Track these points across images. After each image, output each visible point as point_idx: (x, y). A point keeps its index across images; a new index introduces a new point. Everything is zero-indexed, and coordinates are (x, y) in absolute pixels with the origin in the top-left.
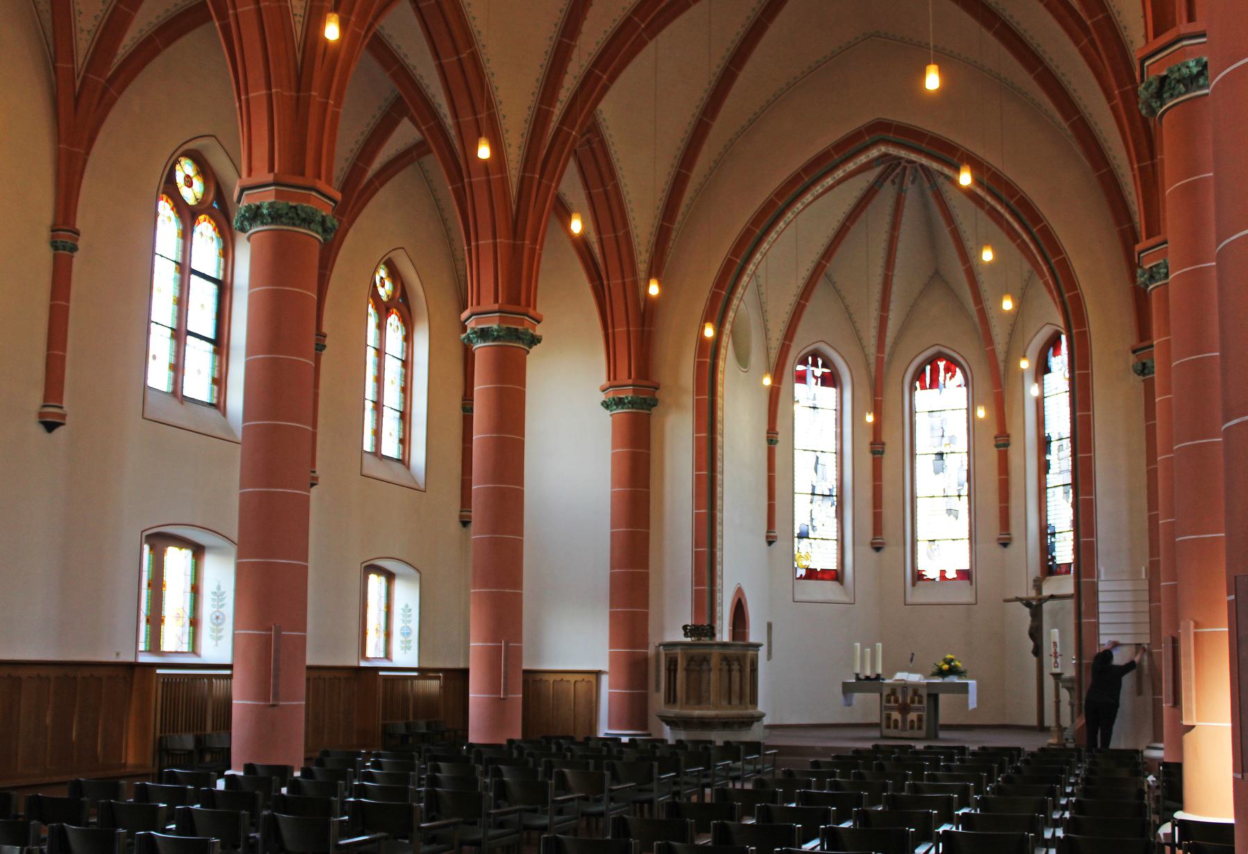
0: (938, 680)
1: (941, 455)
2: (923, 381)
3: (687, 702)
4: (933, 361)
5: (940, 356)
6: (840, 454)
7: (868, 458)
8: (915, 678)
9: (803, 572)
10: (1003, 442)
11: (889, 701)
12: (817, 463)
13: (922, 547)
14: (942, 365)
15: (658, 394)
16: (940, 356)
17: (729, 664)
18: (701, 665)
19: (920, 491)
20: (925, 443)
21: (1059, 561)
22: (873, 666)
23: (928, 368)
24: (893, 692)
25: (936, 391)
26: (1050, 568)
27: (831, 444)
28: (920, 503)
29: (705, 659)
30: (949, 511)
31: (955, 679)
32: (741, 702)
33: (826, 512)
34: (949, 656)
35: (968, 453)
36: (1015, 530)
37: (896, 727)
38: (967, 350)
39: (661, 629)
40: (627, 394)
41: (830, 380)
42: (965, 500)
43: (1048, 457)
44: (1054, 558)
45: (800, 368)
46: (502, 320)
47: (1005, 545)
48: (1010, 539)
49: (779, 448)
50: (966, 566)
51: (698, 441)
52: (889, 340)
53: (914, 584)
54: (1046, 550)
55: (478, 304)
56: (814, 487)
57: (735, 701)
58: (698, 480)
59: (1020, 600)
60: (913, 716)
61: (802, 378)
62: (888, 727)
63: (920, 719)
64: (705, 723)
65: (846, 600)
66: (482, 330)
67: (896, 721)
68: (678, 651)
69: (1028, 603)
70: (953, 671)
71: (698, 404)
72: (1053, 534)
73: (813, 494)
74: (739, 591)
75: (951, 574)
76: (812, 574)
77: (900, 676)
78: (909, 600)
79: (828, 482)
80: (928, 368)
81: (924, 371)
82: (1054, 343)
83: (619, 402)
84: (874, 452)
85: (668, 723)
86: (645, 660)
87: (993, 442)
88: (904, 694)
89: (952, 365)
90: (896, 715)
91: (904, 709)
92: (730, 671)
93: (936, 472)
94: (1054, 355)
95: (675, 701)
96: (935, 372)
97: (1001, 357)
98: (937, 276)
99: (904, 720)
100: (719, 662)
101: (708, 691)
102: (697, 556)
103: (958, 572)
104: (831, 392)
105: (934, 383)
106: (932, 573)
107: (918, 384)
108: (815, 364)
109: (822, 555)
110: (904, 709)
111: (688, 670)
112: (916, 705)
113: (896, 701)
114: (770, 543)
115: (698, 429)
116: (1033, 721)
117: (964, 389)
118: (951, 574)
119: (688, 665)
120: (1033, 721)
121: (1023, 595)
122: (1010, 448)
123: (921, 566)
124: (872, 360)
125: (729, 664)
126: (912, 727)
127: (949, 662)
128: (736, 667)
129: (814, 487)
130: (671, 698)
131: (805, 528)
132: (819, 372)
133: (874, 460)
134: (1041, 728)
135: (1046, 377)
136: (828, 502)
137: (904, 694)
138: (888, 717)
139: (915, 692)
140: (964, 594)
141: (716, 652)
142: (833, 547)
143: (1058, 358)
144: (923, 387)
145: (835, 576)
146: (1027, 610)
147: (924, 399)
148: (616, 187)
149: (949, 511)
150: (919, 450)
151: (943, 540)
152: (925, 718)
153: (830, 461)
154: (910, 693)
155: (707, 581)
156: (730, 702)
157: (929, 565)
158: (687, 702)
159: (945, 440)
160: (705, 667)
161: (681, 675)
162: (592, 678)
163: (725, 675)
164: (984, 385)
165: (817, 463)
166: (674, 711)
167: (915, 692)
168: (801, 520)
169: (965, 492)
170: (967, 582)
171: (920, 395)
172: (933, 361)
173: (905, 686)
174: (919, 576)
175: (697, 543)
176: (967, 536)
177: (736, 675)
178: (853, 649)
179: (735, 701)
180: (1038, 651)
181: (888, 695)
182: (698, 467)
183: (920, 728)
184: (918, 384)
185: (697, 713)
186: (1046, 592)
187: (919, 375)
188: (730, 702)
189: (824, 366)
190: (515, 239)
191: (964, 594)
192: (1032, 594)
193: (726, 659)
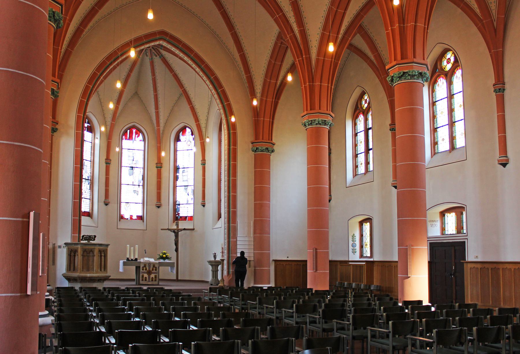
0: (162, 261)
1: (132, 167)
2: (126, 136)
3: (83, 271)
7: (104, 165)
8: (152, 260)
10: (159, 165)
11: (143, 270)
13: (123, 205)
14: (134, 131)
17: (101, 254)
20: (126, 161)
21: (181, 215)
22: (134, 255)
23: (128, 131)
24: (145, 266)
25: (131, 141)
26: (177, 218)
29: (92, 251)
30: (135, 191)
31: (167, 261)
32: (104, 270)
36: (163, 201)
37: (146, 280)
39: (56, 237)
42: (141, 187)
43: (178, 174)
44: (179, 214)
47: (159, 207)
50: (140, 214)
53: (120, 221)
54: (176, 211)
57: (103, 270)
60: (153, 276)
62: (143, 280)
63: (156, 277)
64: (92, 280)
67: (146, 278)
68: (79, 246)
69: (174, 232)
70: (167, 258)
75: (135, 217)
77: (146, 259)
78: (119, 227)
80: (128, 131)
82: (183, 130)
84: (107, 163)
85: (66, 279)
87: (155, 166)
88: (149, 267)
89: (139, 131)
90: (146, 275)
91: (149, 273)
92: (101, 256)
94: (183, 135)
95: (74, 270)
96: (131, 133)
97: (161, 132)
98: (136, 94)
99: (149, 277)
100: (87, 252)
101: (93, 265)
103: (137, 216)
105: (131, 138)
106: (127, 216)
107: (124, 137)
110: (149, 273)
111: (83, 255)
113: (146, 270)
116: (175, 278)
117: (143, 143)
118: (135, 217)
120: (175, 278)
123: (123, 212)
125: (101, 254)
126: (152, 280)
127: (165, 254)
128: (103, 254)
133: (106, 166)
134: (177, 280)
135: (178, 143)
136: (87, 182)
137: (149, 267)
138: (143, 276)
139: (154, 266)
141: (97, 248)
143: (184, 137)
144: (126, 139)
146: (173, 234)
147: (126, 143)
149: (135, 191)
151: (132, 202)
154: (152, 266)
156: (101, 270)
157: (127, 211)
158: (83, 271)
159: (134, 162)
160: (91, 254)
161: (79, 259)
164: (153, 142)
166: (75, 275)
167: (154, 266)
169: (141, 184)
170: (141, 221)
172: (130, 129)
173: (150, 264)
174: (122, 217)
176: (141, 201)
177: (103, 258)
179: (103, 270)
180: (177, 250)
183: (155, 280)
184: (124, 137)
185: (88, 275)
186: (180, 227)
187: (125, 133)
188: (101, 270)
189: (88, 123)
191: (140, 225)
193: (100, 251)
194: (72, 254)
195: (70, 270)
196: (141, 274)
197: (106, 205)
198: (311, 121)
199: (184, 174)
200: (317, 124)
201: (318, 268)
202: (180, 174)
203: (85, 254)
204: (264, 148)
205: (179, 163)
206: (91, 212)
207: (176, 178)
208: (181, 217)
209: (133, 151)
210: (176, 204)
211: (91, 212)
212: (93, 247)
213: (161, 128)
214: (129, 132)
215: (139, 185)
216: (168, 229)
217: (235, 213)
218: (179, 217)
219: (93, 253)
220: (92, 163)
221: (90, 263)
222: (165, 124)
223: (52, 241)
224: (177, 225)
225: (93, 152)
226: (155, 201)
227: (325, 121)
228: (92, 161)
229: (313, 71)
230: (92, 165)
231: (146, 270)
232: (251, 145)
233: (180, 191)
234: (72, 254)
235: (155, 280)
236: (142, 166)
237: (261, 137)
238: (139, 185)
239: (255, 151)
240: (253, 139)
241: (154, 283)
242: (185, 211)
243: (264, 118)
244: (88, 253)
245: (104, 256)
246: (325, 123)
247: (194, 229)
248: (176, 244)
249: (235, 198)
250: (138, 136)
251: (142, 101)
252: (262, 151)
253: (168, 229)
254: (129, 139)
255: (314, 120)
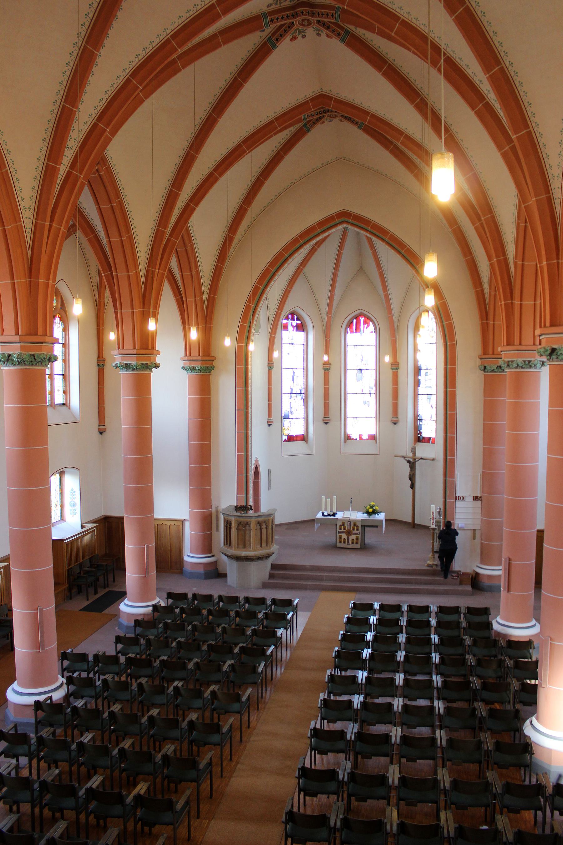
1: (361, 370)
3: (238, 547)
4: (357, 317)
5: (361, 315)
6: (306, 369)
9: (286, 437)
10: (395, 366)
11: (340, 529)
12: (294, 376)
13: (349, 421)
14: (362, 319)
15: (215, 363)
16: (361, 315)
18: (245, 526)
19: (349, 390)
20: (353, 362)
23: (355, 321)
24: (343, 524)
25: (358, 335)
26: (419, 439)
27: (300, 364)
28: (349, 396)
29: (247, 524)
30: (365, 402)
32: (267, 546)
33: (298, 402)
34: (372, 503)
35: (376, 370)
36: (401, 416)
37: (344, 542)
38: (377, 313)
40: (198, 365)
41: (301, 327)
42: (373, 396)
43: (419, 378)
44: (421, 433)
45: (285, 321)
46: (138, 359)
48: (398, 421)
49: (274, 371)
50: (373, 432)
51: (238, 392)
52: (334, 306)
53: (345, 442)
54: (417, 429)
55: (123, 348)
56: (292, 390)
58: (238, 414)
59: (404, 457)
60: (353, 537)
61: (286, 327)
62: (340, 542)
63: (357, 539)
65: (308, 451)
66: (126, 364)
67: (344, 539)
69: (409, 462)
71: (238, 371)
72: (421, 420)
73: (291, 393)
74: (257, 461)
75: (365, 437)
76: (291, 438)
79: (299, 386)
80: (355, 321)
81: (352, 322)
83: (194, 369)
86: (210, 515)
89: (368, 319)
90: (344, 536)
91: (349, 533)
92: (261, 529)
93: (358, 380)
95: (230, 545)
96: (358, 323)
97: (395, 320)
98: (361, 270)
101: (250, 540)
102: (238, 457)
103: (369, 436)
104: (301, 334)
105: (358, 330)
107: (349, 329)
108: (293, 319)
109: (295, 427)
110: (349, 533)
111: (238, 530)
112: (355, 531)
113: (345, 529)
114: (269, 425)
115: (238, 385)
117: (374, 334)
118: (365, 437)
119: (238, 527)
121: (404, 455)
122: (399, 370)
123: (349, 432)
124: (324, 316)
126: (353, 543)
128: (264, 526)
129: (292, 390)
130: (228, 541)
131: (287, 413)
132: (295, 323)
136: (299, 397)
138: (340, 537)
139: (355, 525)
140: (371, 448)
141: (253, 521)
142: (302, 422)
144: (352, 332)
145: (303, 438)
147: (352, 338)
148: (192, 246)
149: (365, 402)
150: (349, 367)
151: (361, 418)
152: (360, 538)
153: (300, 374)
154: (352, 525)
155: (244, 471)
156: (261, 546)
160: (247, 527)
161: (234, 532)
162: (180, 524)
163: (259, 532)
165: (294, 376)
167: (355, 525)
168: (285, 409)
169: (373, 392)
170: (374, 441)
171: (349, 335)
172: (357, 317)
174: (348, 438)
175: (238, 450)
176: (374, 416)
177: (264, 531)
178: (321, 499)
180: (413, 486)
181: (341, 525)
182: (238, 407)
183: (357, 543)
184: (349, 329)
185: (244, 553)
186: (419, 454)
187: (350, 324)
188: (261, 546)
189: (298, 319)
190: (144, 308)
192: (411, 455)
194: (228, 526)
195: (227, 544)
196: (338, 535)
197: (326, 423)
198: (509, 361)
199: (427, 377)
200: (516, 368)
201: (512, 588)
202: (421, 378)
203: (241, 527)
204: (494, 367)
205: (422, 363)
206: (305, 434)
207: (417, 383)
208: (424, 438)
209: (362, 347)
210: (417, 419)
211: (305, 434)
212: (248, 519)
213: (395, 315)
214: (353, 323)
215: (370, 394)
216: (404, 457)
217: (453, 462)
218: (421, 438)
219: (250, 526)
220: (305, 371)
221: (247, 538)
222: (401, 307)
223: (214, 503)
224: (414, 453)
225: (305, 356)
226: (390, 416)
227: (529, 362)
228: (305, 368)
229: (513, 280)
230: (305, 373)
231: (345, 529)
232: (478, 362)
233: (422, 400)
234: (228, 525)
235: (357, 543)
236: (374, 368)
237: (491, 351)
238: (370, 394)
239: (484, 370)
240: (479, 351)
241: (355, 546)
242: (429, 429)
243: (494, 321)
244: (243, 526)
245: (266, 528)
246: (529, 364)
247: (433, 460)
248: (412, 477)
249: (453, 439)
250: (368, 326)
251: (370, 279)
252: (493, 371)
253: (402, 456)
254: (356, 332)
255: (512, 361)
